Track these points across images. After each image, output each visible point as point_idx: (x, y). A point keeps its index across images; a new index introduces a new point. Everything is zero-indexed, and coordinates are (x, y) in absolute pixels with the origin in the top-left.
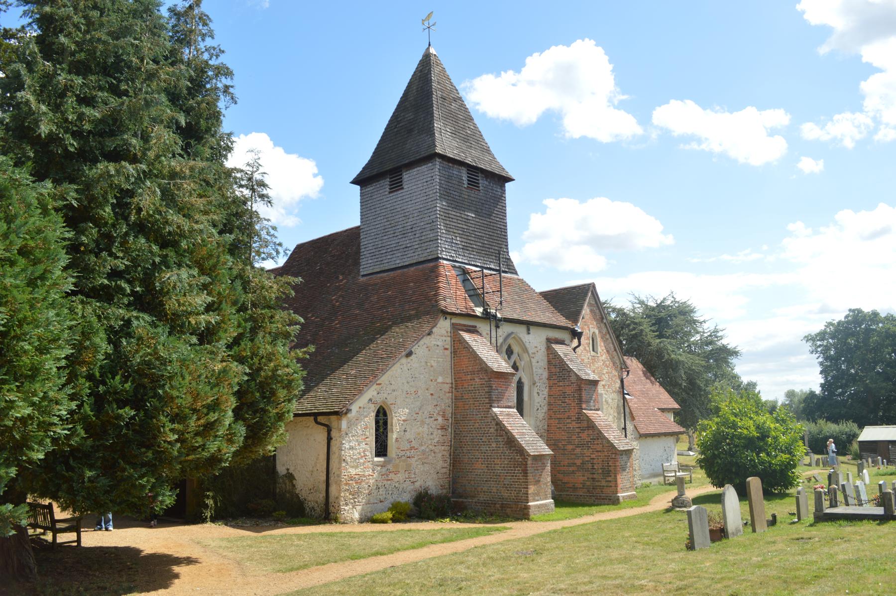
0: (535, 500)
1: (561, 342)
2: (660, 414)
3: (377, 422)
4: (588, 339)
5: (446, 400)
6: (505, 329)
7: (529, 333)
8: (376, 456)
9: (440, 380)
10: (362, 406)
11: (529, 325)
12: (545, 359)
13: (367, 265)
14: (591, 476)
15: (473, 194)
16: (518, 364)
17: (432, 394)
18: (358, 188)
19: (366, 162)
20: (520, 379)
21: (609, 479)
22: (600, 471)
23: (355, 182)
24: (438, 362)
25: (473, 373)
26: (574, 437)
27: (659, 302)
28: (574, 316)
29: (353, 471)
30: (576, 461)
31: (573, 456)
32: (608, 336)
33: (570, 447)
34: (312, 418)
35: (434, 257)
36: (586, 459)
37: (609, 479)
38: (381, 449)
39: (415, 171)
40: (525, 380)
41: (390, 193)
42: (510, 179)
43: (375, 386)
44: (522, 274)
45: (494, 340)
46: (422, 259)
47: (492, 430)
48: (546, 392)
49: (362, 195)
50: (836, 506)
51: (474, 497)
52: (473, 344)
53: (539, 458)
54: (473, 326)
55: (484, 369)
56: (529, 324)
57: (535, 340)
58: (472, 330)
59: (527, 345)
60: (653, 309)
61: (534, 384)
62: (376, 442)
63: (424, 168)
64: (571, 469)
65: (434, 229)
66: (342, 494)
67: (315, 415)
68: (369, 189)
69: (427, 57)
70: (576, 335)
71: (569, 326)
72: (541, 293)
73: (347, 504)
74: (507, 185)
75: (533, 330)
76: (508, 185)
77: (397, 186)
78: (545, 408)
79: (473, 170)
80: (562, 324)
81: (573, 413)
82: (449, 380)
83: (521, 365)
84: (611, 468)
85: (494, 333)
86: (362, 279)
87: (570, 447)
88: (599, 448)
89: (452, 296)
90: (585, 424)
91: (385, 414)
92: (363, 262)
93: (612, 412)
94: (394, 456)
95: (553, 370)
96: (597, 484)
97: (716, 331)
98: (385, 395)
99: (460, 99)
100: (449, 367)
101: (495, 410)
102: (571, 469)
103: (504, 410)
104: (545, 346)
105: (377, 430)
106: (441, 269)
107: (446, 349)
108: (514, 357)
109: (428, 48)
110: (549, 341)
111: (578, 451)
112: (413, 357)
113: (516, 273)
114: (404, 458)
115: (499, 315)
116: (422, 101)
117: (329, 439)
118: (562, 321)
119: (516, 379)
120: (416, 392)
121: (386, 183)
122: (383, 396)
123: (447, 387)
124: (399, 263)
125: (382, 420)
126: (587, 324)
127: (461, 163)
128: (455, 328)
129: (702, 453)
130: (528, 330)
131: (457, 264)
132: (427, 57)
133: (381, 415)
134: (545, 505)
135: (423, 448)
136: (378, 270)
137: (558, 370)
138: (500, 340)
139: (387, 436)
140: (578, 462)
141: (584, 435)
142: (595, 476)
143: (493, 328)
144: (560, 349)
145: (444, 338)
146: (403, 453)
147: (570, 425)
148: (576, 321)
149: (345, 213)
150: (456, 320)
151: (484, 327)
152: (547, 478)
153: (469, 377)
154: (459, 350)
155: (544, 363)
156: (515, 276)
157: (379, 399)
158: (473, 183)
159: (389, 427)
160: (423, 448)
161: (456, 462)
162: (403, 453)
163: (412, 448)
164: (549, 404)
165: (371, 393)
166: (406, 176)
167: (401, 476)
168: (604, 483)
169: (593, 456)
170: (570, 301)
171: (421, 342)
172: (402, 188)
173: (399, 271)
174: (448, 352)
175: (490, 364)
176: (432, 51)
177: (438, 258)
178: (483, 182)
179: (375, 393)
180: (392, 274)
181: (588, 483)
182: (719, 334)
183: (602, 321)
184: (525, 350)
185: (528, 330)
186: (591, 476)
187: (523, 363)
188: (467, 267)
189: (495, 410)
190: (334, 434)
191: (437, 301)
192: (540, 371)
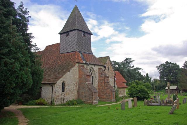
0: (94, 101)
3: (62, 85)
11: (95, 65)
15: (84, 37)
19: (62, 29)
38: (63, 90)
39: (72, 32)
42: (92, 34)
59: (94, 69)
63: (74, 32)
68: (62, 35)
70: (105, 67)
75: (96, 66)
76: (92, 36)
77: (68, 35)
79: (84, 32)
90: (105, 86)
91: (64, 83)
112: (70, 72)
115: (89, 63)
117: (52, 88)
119: (92, 76)
121: (66, 34)
122: (64, 80)
124: (68, 51)
129: (129, 91)
140: (104, 93)
141: (105, 88)
143: (87, 65)
149: (56, 39)
150: (79, 64)
158: (84, 35)
164: (99, 81)
165: (61, 79)
174: (78, 71)
178: (86, 35)
180: (67, 54)
190: (53, 87)
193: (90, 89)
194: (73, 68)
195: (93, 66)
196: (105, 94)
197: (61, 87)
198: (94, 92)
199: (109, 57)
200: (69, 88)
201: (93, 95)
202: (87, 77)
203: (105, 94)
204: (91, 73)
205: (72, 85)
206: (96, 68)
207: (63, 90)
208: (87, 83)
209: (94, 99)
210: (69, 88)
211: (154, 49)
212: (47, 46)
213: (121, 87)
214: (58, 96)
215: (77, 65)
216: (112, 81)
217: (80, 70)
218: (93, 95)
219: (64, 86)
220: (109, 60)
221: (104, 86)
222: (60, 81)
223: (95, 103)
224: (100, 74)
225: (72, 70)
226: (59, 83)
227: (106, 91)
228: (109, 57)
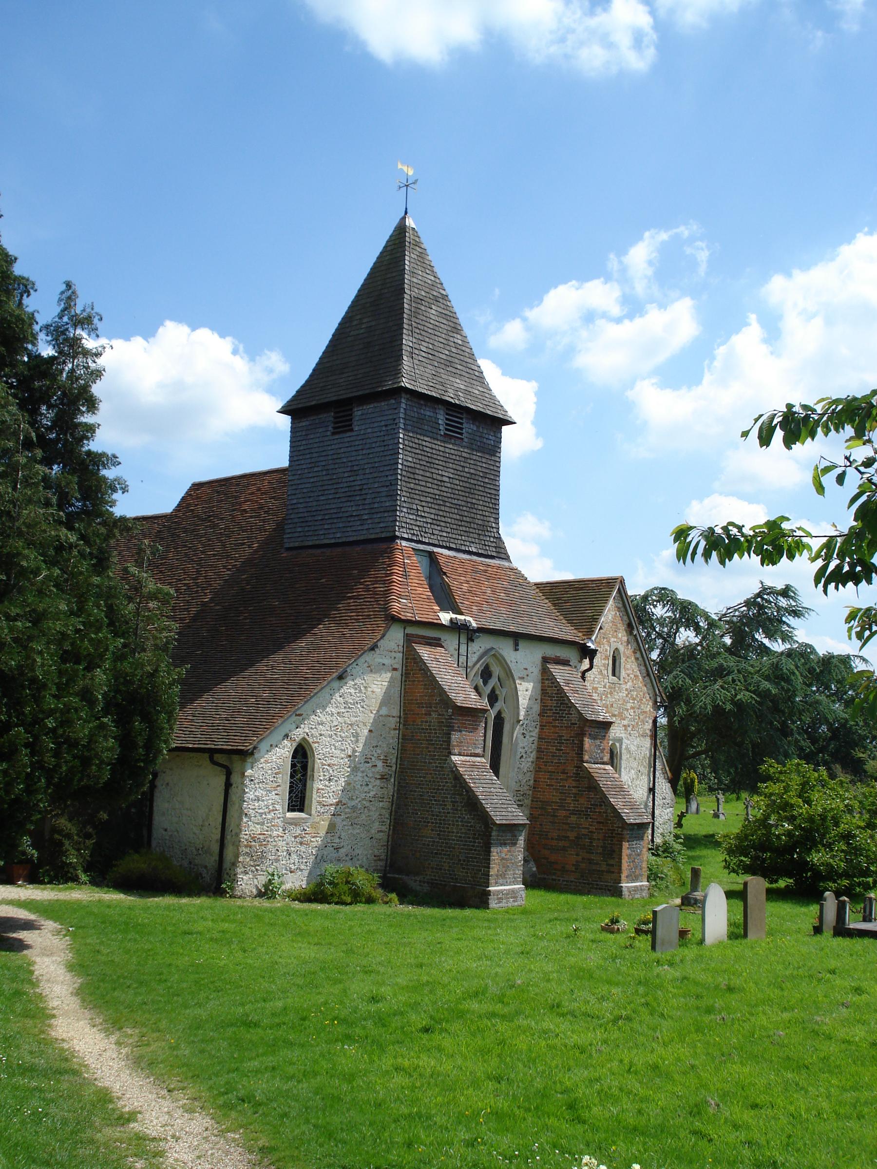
1: (565, 663)
4: (607, 658)
6: (480, 645)
7: (516, 650)
11: (517, 638)
16: (497, 692)
19: (303, 382)
20: (499, 713)
21: (611, 862)
22: (600, 850)
26: (569, 800)
28: (589, 624)
29: (258, 829)
30: (569, 834)
33: (562, 813)
34: (207, 755)
35: (388, 535)
36: (584, 831)
37: (611, 862)
39: (369, 408)
41: (333, 434)
44: (516, 563)
45: (463, 659)
46: (373, 536)
48: (535, 733)
49: (294, 430)
50: (870, 921)
52: (432, 666)
53: (511, 829)
54: (435, 639)
55: (445, 701)
56: (517, 638)
57: (524, 662)
58: (435, 643)
59: (512, 666)
64: (561, 844)
65: (393, 496)
66: (241, 859)
67: (212, 752)
69: (401, 230)
71: (577, 640)
72: (541, 587)
73: (246, 873)
74: (504, 428)
75: (522, 644)
76: (505, 429)
77: (344, 425)
78: (533, 755)
79: (456, 410)
80: (569, 638)
82: (396, 713)
83: (501, 693)
85: (463, 648)
87: (562, 813)
89: (411, 596)
93: (635, 765)
95: (549, 703)
96: (594, 867)
99: (445, 297)
100: (397, 695)
101: (454, 758)
102: (561, 844)
103: (468, 758)
104: (540, 667)
105: (292, 776)
106: (398, 556)
108: (493, 682)
109: (404, 218)
110: (545, 660)
111: (573, 819)
113: (507, 558)
115: (474, 624)
116: (388, 303)
117: (228, 785)
118: (568, 632)
119: (493, 714)
121: (329, 417)
124: (340, 537)
126: (610, 633)
128: (409, 640)
132: (401, 230)
134: (513, 891)
135: (353, 803)
137: (554, 702)
138: (473, 659)
140: (572, 835)
143: (463, 640)
144: (559, 673)
145: (393, 654)
148: (589, 633)
150: (410, 630)
151: (451, 641)
152: (518, 852)
153: (423, 711)
154: (414, 673)
156: (506, 564)
159: (309, 773)
164: (539, 750)
168: (604, 867)
169: (593, 828)
171: (361, 661)
172: (352, 430)
173: (339, 550)
175: (452, 696)
176: (410, 222)
177: (394, 538)
178: (468, 427)
180: (328, 551)
181: (583, 865)
188: (436, 550)
189: (454, 758)
190: (235, 778)
191: (387, 602)
195: (505, 649)
197: (284, 781)
204: (487, 690)
216: (633, 748)
223: (500, 900)
226: (272, 762)
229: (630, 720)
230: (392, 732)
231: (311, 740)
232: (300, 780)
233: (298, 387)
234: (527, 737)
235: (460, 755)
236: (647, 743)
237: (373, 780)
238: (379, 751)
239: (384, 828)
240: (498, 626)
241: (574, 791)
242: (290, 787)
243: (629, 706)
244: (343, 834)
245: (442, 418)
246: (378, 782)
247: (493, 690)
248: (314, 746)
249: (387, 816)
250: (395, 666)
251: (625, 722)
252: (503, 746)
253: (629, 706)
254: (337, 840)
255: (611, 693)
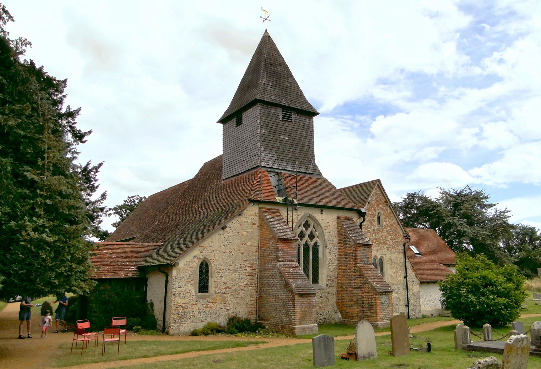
2: (444, 267)
3: (200, 271)
5: (254, 256)
7: (322, 214)
8: (199, 292)
9: (249, 244)
10: (188, 260)
11: (322, 208)
12: (336, 230)
13: (226, 173)
14: (362, 309)
17: (242, 253)
18: (221, 125)
20: (316, 243)
21: (372, 311)
22: (367, 306)
23: (221, 121)
24: (248, 232)
25: (269, 239)
26: (352, 282)
27: (458, 192)
29: (181, 301)
31: (352, 295)
32: (392, 215)
37: (372, 311)
38: (203, 287)
40: (320, 243)
41: (236, 127)
42: (316, 114)
43: (198, 248)
47: (278, 277)
48: (336, 252)
51: (268, 320)
60: (453, 197)
61: (326, 247)
62: (199, 284)
63: (251, 110)
64: (350, 303)
66: (172, 316)
68: (227, 125)
70: (362, 215)
73: (175, 323)
75: (324, 210)
76: (315, 118)
77: (239, 122)
78: (336, 263)
79: (286, 109)
81: (352, 266)
82: (256, 244)
84: (373, 304)
86: (223, 182)
87: (350, 289)
88: (366, 290)
90: (358, 274)
91: (207, 266)
92: (224, 171)
94: (213, 292)
95: (341, 237)
96: (365, 314)
97: (505, 212)
98: (207, 254)
102: (350, 303)
105: (200, 276)
107: (254, 224)
110: (339, 218)
111: (354, 291)
112: (227, 229)
114: (220, 294)
115: (296, 202)
117: (167, 282)
120: (230, 252)
121: (234, 121)
123: (254, 249)
124: (240, 170)
125: (204, 270)
127: (276, 105)
130: (322, 211)
131: (272, 170)
133: (204, 266)
135: (235, 287)
136: (230, 176)
139: (208, 280)
140: (355, 299)
141: (358, 281)
142: (364, 309)
145: (253, 217)
146: (220, 291)
147: (350, 274)
150: (261, 206)
155: (335, 232)
157: (202, 256)
158: (287, 119)
159: (210, 274)
160: (235, 287)
161: (260, 297)
162: (220, 291)
163: (226, 288)
166: (244, 115)
167: (218, 306)
168: (369, 314)
169: (363, 295)
170: (368, 192)
174: (256, 227)
178: (294, 117)
179: (199, 252)
180: (232, 179)
181: (360, 314)
182: (507, 214)
183: (387, 205)
184: (319, 224)
185: (322, 211)
186: (362, 309)
187: (317, 233)
190: (169, 277)
192: (331, 238)
193: (287, 285)
194: (239, 219)
195: (316, 214)
196: (356, 303)
198: (301, 295)
199: (379, 181)
200: (223, 279)
201: (294, 305)
202: (281, 246)
203: (356, 303)
205: (235, 271)
206: (328, 221)
207: (203, 287)
208: (279, 263)
209: (298, 317)
210: (223, 279)
211: (4, 6)
212: (206, 164)
213: (425, 280)
214: (184, 307)
215: (252, 211)
216: (393, 258)
217: (262, 224)
218: (296, 303)
219: (207, 275)
220: (379, 192)
221: (352, 274)
222: (189, 257)
224: (343, 238)
225: (234, 225)
227: (360, 293)
228: (379, 181)
229: (390, 245)
230: (255, 253)
231: (209, 259)
232: (205, 277)
233: (225, 111)
234: (332, 254)
235: (283, 261)
236: (401, 256)
237: (245, 276)
238: (248, 263)
239: (253, 299)
240: (310, 202)
241: (354, 278)
242: (199, 281)
243: (389, 239)
244: (231, 302)
245: (280, 113)
246: (248, 277)
247: (311, 233)
248: (212, 261)
249: (255, 293)
250: (254, 222)
251: (387, 246)
252: (320, 260)
253: (389, 239)
254: (228, 305)
255: (378, 233)
